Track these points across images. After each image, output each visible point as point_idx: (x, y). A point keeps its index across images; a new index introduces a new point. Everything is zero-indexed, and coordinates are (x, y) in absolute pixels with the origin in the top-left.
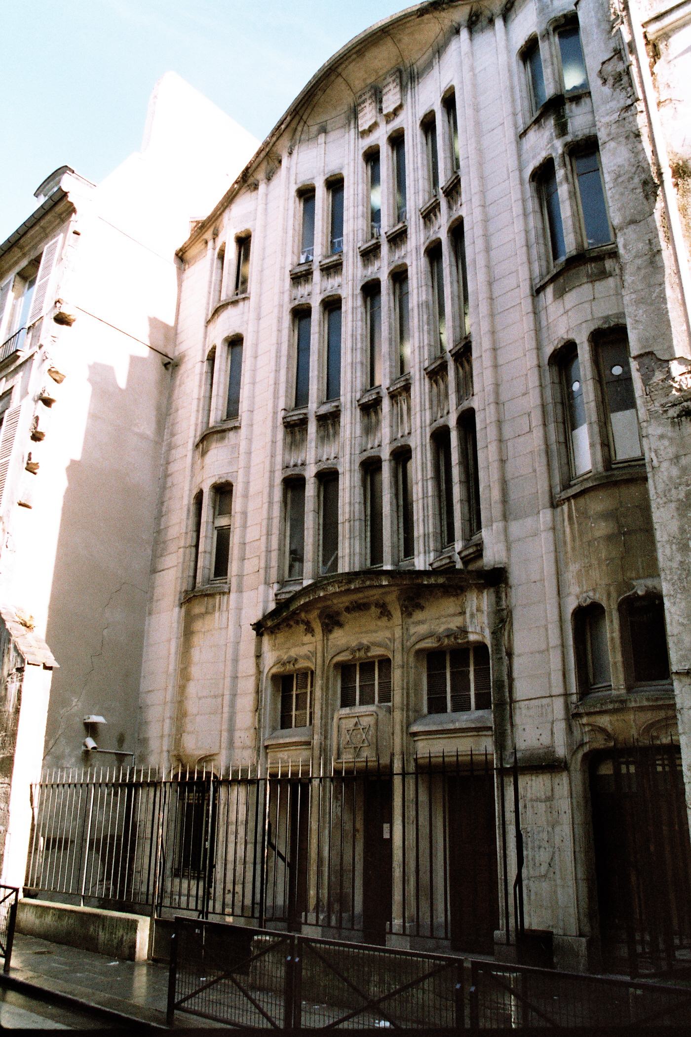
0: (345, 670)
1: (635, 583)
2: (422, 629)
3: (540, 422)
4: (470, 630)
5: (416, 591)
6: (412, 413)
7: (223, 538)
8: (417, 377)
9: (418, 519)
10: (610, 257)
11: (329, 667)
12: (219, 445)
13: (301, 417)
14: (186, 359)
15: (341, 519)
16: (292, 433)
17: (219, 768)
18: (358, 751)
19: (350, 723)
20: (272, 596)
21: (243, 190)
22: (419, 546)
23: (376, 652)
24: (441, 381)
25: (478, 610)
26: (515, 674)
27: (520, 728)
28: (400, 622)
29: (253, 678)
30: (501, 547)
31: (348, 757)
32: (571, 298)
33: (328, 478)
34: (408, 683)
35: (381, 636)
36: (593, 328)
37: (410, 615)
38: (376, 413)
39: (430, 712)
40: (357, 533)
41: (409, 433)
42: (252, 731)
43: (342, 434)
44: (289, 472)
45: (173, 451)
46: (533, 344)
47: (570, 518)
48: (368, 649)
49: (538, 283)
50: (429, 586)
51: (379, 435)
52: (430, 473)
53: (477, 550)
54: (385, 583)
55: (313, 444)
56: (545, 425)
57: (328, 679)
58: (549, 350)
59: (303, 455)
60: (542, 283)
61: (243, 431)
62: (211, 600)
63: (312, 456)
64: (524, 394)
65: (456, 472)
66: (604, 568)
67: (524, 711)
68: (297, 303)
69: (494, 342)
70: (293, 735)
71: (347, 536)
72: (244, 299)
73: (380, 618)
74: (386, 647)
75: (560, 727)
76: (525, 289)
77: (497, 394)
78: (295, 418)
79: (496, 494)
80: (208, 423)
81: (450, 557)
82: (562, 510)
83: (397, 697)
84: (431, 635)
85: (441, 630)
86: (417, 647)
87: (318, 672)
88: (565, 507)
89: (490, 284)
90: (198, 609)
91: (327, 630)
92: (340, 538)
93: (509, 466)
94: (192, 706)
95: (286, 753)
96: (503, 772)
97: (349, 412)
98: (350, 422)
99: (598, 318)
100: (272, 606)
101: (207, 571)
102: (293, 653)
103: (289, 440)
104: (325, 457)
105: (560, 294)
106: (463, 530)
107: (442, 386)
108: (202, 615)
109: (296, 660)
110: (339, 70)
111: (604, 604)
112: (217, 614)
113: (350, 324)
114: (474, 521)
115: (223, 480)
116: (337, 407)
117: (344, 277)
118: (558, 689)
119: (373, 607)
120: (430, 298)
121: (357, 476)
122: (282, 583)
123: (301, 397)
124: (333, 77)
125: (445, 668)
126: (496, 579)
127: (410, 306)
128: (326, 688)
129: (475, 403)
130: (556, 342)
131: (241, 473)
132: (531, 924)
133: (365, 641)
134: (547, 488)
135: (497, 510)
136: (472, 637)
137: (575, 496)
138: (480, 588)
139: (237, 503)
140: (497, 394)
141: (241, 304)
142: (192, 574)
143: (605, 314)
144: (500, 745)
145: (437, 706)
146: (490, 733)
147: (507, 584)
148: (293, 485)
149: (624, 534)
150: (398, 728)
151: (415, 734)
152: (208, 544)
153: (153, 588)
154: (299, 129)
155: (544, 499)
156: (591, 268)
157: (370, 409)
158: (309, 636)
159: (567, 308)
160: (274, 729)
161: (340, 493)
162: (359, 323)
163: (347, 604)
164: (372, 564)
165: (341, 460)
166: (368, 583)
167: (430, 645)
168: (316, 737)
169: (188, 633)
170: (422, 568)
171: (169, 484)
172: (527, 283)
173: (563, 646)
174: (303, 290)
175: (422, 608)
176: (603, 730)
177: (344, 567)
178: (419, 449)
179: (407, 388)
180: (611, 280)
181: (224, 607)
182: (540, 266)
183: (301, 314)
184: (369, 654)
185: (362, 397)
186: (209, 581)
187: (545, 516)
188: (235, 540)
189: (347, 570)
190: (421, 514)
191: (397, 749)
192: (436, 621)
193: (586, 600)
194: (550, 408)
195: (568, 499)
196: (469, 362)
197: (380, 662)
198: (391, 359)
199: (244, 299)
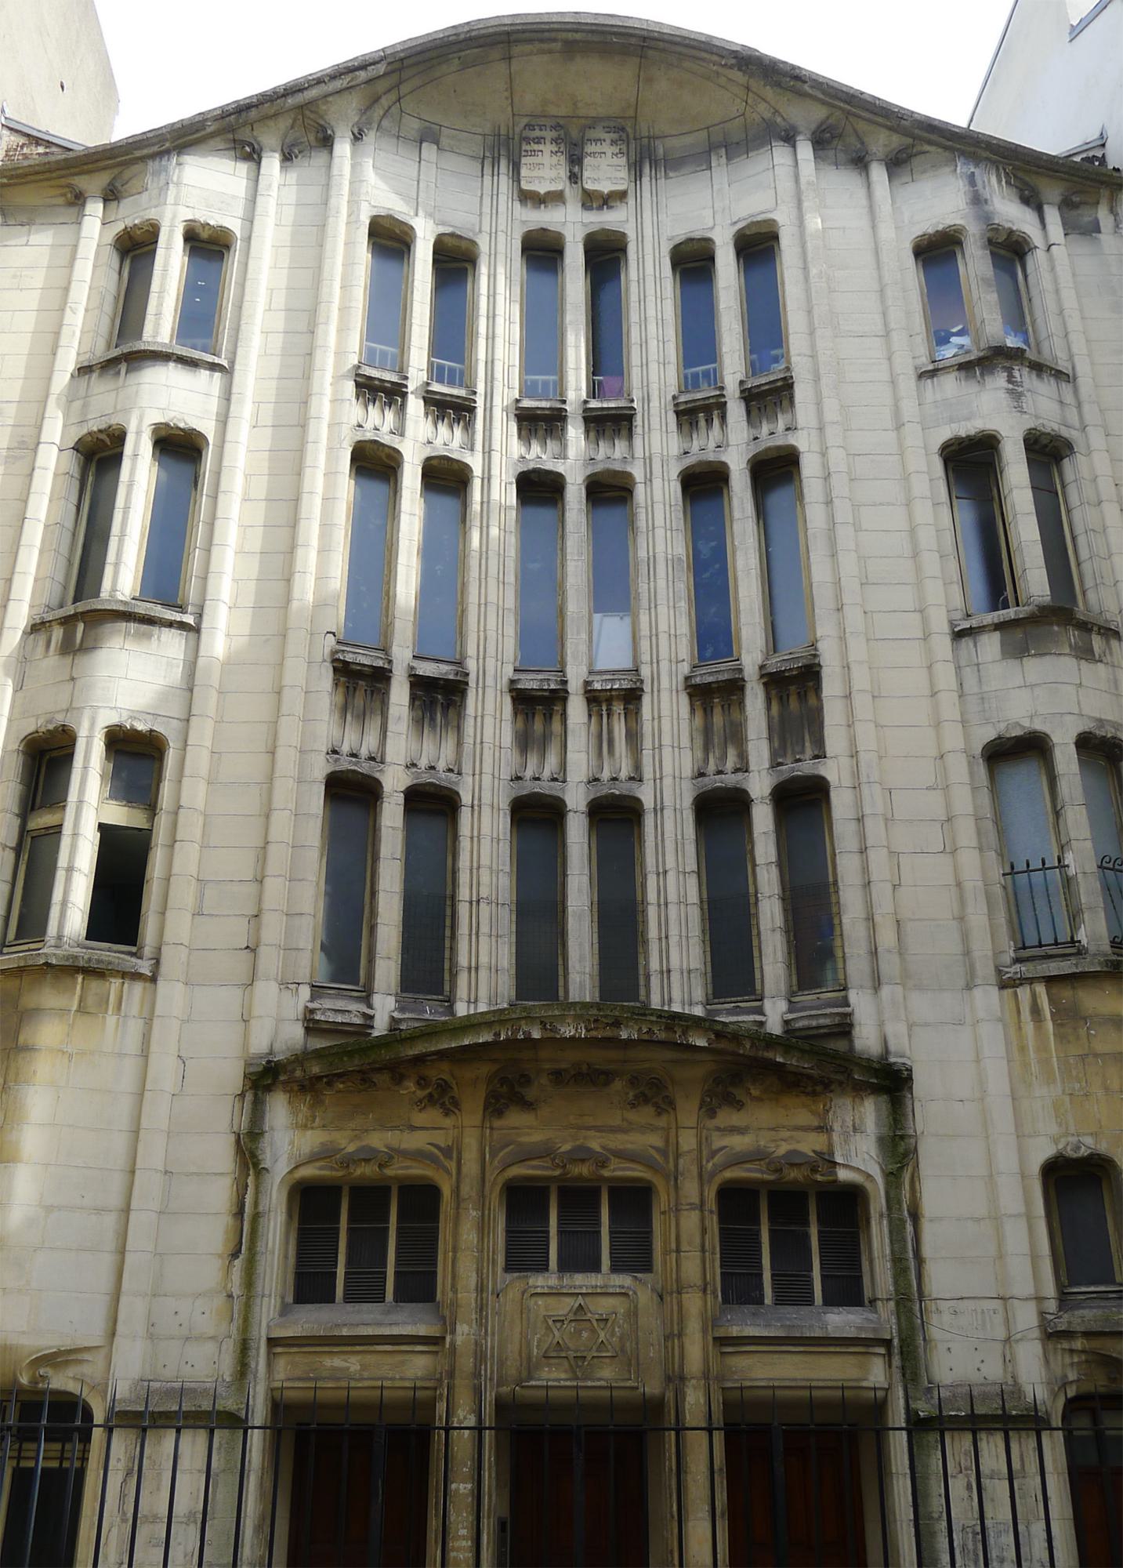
2: (739, 1143)
4: (839, 1159)
5: (746, 1068)
10: (1099, 633)
11: (494, 1183)
21: (217, 142)
24: (717, 711)
25: (855, 1130)
26: (927, 1251)
27: (941, 1348)
28: (692, 1122)
30: (902, 1028)
35: (648, 1141)
36: (1081, 729)
37: (712, 1113)
38: (548, 717)
42: (220, 1300)
47: (1036, 1011)
48: (603, 1164)
62: (95, 985)
67: (947, 1318)
73: (633, 1106)
86: (728, 1174)
88: (1024, 993)
91: (495, 1106)
95: (354, 1359)
102: (378, 1140)
103: (339, 698)
105: (1016, 651)
107: (718, 719)
110: (516, 50)
112: (111, 1020)
118: (1023, 1285)
119: (618, 1085)
124: (496, 54)
125: (757, 1222)
128: (483, 1228)
129: (833, 771)
130: (1002, 726)
136: (843, 1175)
138: (860, 1089)
146: (882, 1351)
150: (694, 1326)
151: (722, 1341)
154: (385, 102)
155: (985, 970)
156: (1073, 635)
163: (563, 1066)
167: (758, 1175)
175: (739, 1105)
183: (374, 464)
184: (606, 1173)
192: (765, 1134)
193: (1079, 1148)
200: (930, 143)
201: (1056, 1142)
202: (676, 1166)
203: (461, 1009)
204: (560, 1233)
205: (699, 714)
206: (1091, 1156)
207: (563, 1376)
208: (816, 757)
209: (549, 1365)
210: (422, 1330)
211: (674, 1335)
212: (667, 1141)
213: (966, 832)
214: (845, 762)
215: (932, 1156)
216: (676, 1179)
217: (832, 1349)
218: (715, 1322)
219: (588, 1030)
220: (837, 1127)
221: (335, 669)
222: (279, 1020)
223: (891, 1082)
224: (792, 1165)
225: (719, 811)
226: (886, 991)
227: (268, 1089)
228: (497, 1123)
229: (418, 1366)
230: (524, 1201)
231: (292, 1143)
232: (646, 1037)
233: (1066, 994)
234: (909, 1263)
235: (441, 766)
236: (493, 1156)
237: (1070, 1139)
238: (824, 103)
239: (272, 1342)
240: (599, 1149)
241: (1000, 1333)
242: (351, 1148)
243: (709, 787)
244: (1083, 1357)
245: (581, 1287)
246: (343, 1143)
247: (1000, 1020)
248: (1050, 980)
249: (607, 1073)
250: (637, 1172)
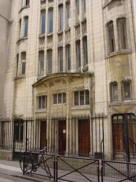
0: (55, 95)
1: (125, 77)
2: (74, 86)
3: (103, 39)
5: (73, 77)
6: (71, 36)
7: (24, 65)
8: (72, 28)
9: (72, 61)
12: (23, 43)
13: (43, 36)
14: (13, 22)
15: (53, 61)
16: (41, 40)
17: (25, 117)
18: (58, 114)
19: (56, 108)
20: (36, 78)
22: (72, 67)
23: (62, 91)
25: (87, 82)
29: (32, 97)
30: (93, 68)
31: (56, 115)
32: (112, 10)
33: (50, 51)
34: (70, 99)
35: (64, 88)
38: (62, 36)
39: (75, 105)
40: (57, 64)
41: (70, 41)
42: (32, 109)
43: (53, 41)
44: (40, 50)
45: (11, 44)
46: (102, 21)
47: (110, 62)
49: (104, 6)
50: (75, 76)
51: (62, 41)
52: (75, 51)
53: (87, 69)
54: (65, 75)
55: (46, 43)
56: (104, 40)
57: (50, 98)
58: (106, 23)
59: (44, 45)
60: (105, 6)
61: (29, 40)
62: (21, 80)
63: (46, 46)
64: (99, 33)
65: (82, 51)
66: (118, 74)
67: (97, 105)
68: (42, 8)
69: (92, 20)
70: (42, 110)
71: (55, 65)
72: (28, 7)
73: (63, 84)
74: (65, 91)
75: (106, 109)
76: (101, 8)
77: (93, 32)
78: (42, 37)
79: (92, 56)
80: (20, 37)
81: (80, 70)
82: (108, 60)
83: (68, 101)
84: (76, 88)
85: (78, 86)
86: (72, 90)
87: (48, 96)
88: (109, 59)
89: (92, 6)
90: (18, 81)
92: (53, 65)
93: (95, 49)
94: (17, 104)
96: (92, 118)
97: (55, 35)
98: (55, 38)
99: (119, 15)
100: (36, 81)
101: (20, 73)
102: (42, 91)
103: (40, 42)
104: (49, 46)
105: (109, 9)
106: (83, 64)
108: (19, 83)
109: (42, 93)
111: (117, 82)
112: (23, 83)
113: (55, 15)
114: (86, 61)
115: (24, 51)
116: (52, 34)
117: (54, 3)
118: (106, 100)
119: (61, 81)
120: (76, 9)
121: (57, 51)
122: (39, 75)
123: (43, 31)
126: (91, 75)
127: (71, 10)
128: (50, 100)
129: (87, 34)
131: (28, 49)
132: (98, 151)
134: (104, 55)
135: (92, 60)
136: (86, 88)
137: (111, 57)
138: (88, 77)
139: (27, 57)
140: (93, 32)
141: (28, 8)
142: (16, 73)
143: (120, 14)
144: (92, 113)
145: (76, 104)
147: (94, 76)
148: (41, 52)
149: (123, 66)
151: (72, 110)
152: (20, 66)
153: (6, 77)
155: (104, 57)
157: (60, 35)
158: (46, 88)
159: (111, 12)
160: (37, 109)
161: (53, 55)
162: (58, 14)
163: (55, 80)
164: (60, 71)
165: (53, 47)
166: (61, 75)
167: (75, 90)
168: (48, 111)
169: (16, 87)
170: (73, 72)
171: (10, 52)
172: (101, 6)
173: (107, 91)
174: (43, 5)
175: (73, 82)
176: (116, 110)
177: (54, 72)
178: (72, 45)
179: (69, 30)
180: (122, 6)
181: (24, 81)
182: (104, 2)
183: (43, 11)
184: (61, 92)
185: (58, 32)
186: (20, 75)
187: (104, 61)
188: (27, 65)
189: (54, 73)
190: (73, 60)
191: (68, 113)
192: (77, 85)
194: (106, 36)
195: (109, 58)
196: (86, 25)
197: (63, 94)
198: (65, 23)
199: (28, 7)
204: (58, 99)
205: (76, 30)
206: (114, 81)
210: (45, 111)
213: (102, 39)
215: (96, 84)
218: (70, 108)
220: (85, 82)
221: (39, 39)
222: (35, 80)
223: (91, 75)
224: (79, 88)
225: (78, 42)
226: (91, 63)
227: (34, 87)
228: (51, 88)
229: (45, 115)
230: (55, 95)
233: (113, 58)
234: (93, 99)
235: (51, 46)
239: (36, 113)
241: (103, 107)
247: (106, 64)
249: (59, 80)
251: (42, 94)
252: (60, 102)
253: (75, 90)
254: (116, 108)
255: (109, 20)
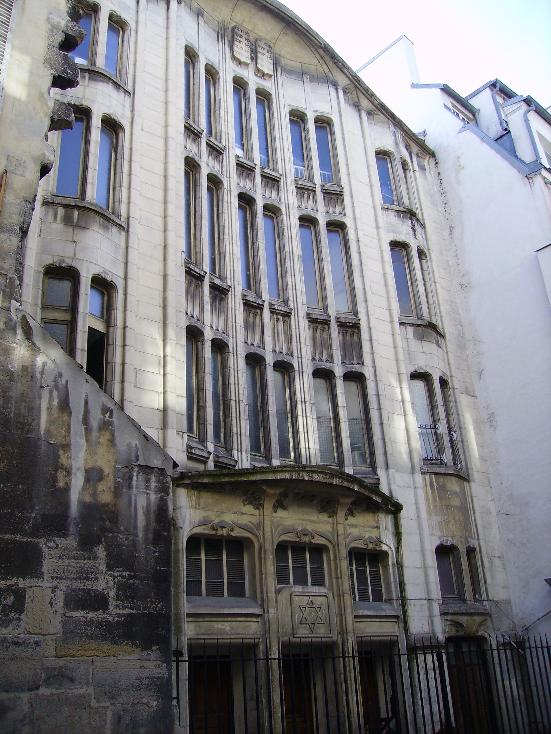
2: (355, 532)
18: (312, 627)
24: (318, 331)
25: (386, 529)
31: (303, 633)
54: (356, 489)
67: (413, 607)
88: (427, 477)
95: (227, 624)
96: (413, 650)
102: (229, 518)
119: (315, 502)
133: (309, 528)
136: (384, 548)
167: (360, 546)
193: (447, 542)
200: (382, 112)
201: (440, 538)
202: (338, 540)
203: (276, 462)
207: (307, 632)
208: (359, 364)
209: (302, 627)
211: (341, 614)
212: (333, 528)
214: (372, 370)
216: (338, 545)
217: (387, 620)
219: (324, 479)
223: (394, 508)
226: (391, 471)
229: (252, 629)
231: (190, 515)
232: (341, 484)
236: (275, 531)
237: (445, 538)
238: (349, 79)
239: (189, 615)
240: (310, 530)
242: (217, 521)
243: (320, 367)
244: (450, 623)
245: (311, 592)
246: (213, 518)
248: (436, 474)
250: (323, 541)
251: (232, 530)
252: (301, 580)
253: (359, 544)
254: (463, 619)
255: (421, 368)
